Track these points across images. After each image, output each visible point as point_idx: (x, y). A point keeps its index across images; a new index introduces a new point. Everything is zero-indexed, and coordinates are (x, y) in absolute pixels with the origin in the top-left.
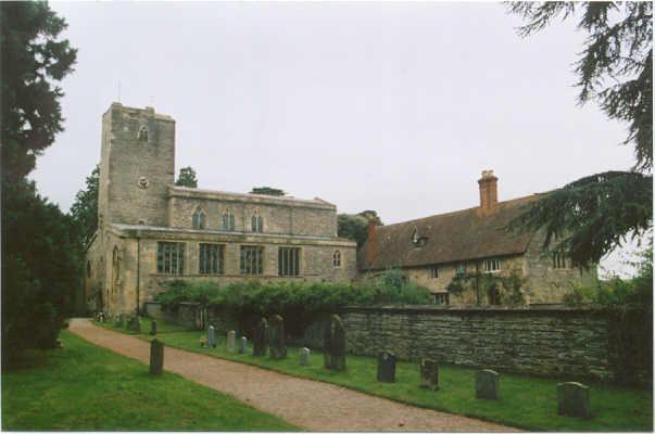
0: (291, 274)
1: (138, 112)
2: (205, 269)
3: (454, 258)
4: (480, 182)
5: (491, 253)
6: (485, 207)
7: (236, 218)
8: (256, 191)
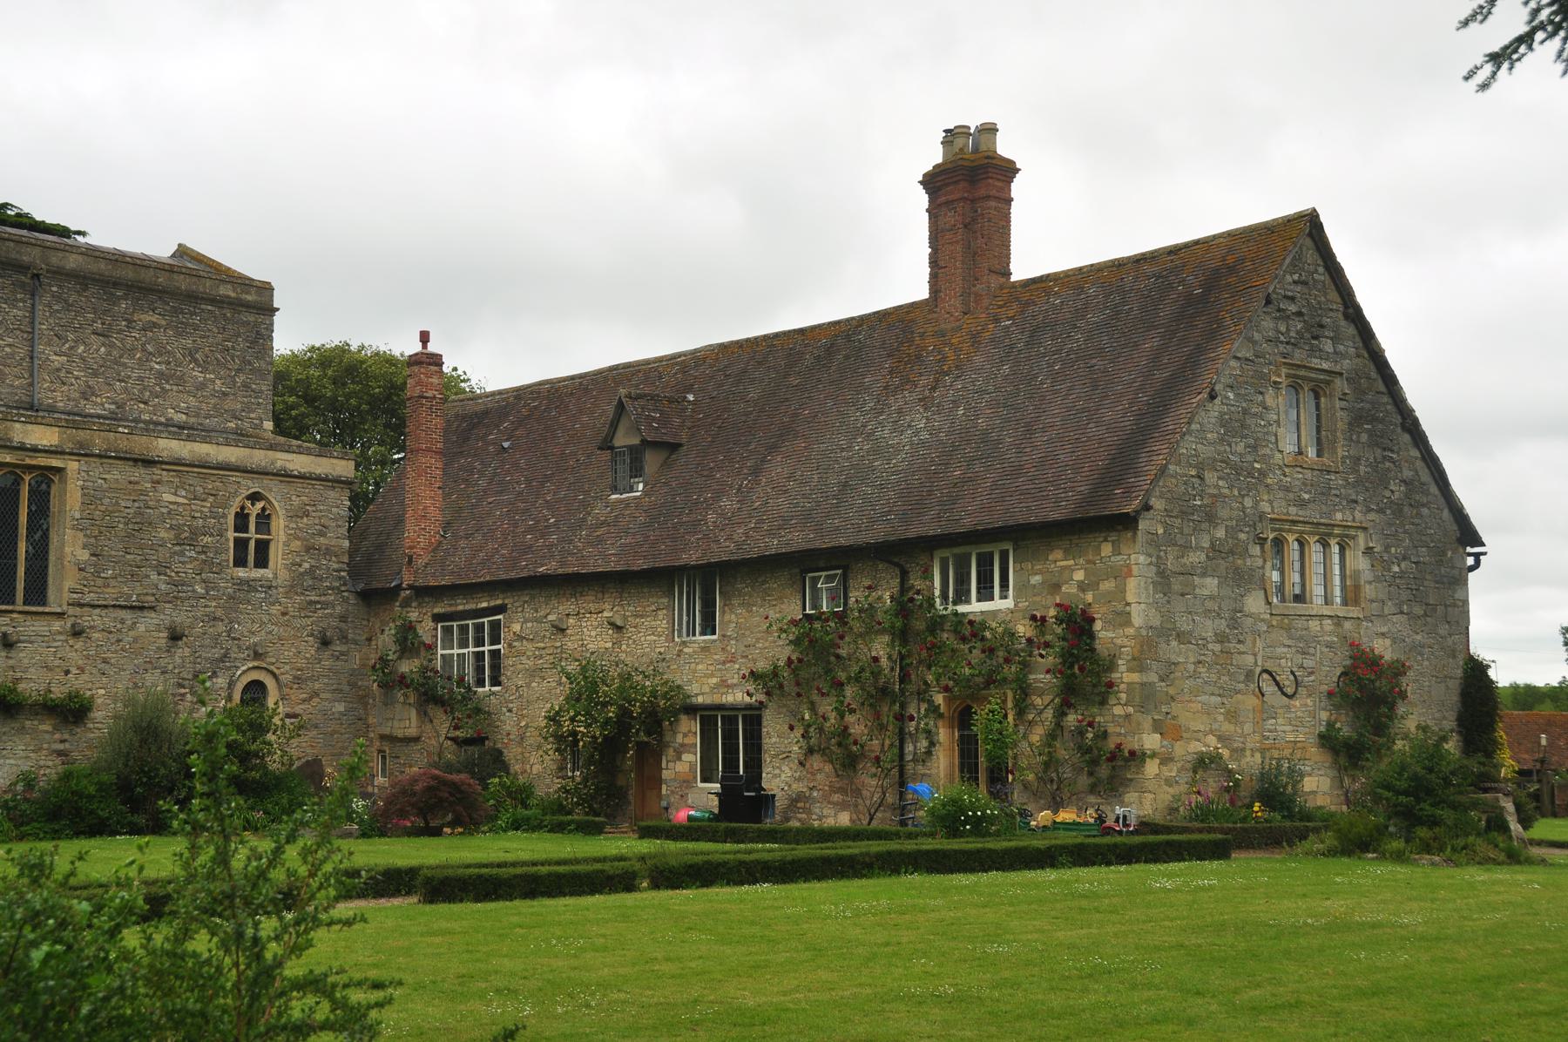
3: (797, 539)
4: (932, 182)
5: (968, 517)
6: (953, 303)
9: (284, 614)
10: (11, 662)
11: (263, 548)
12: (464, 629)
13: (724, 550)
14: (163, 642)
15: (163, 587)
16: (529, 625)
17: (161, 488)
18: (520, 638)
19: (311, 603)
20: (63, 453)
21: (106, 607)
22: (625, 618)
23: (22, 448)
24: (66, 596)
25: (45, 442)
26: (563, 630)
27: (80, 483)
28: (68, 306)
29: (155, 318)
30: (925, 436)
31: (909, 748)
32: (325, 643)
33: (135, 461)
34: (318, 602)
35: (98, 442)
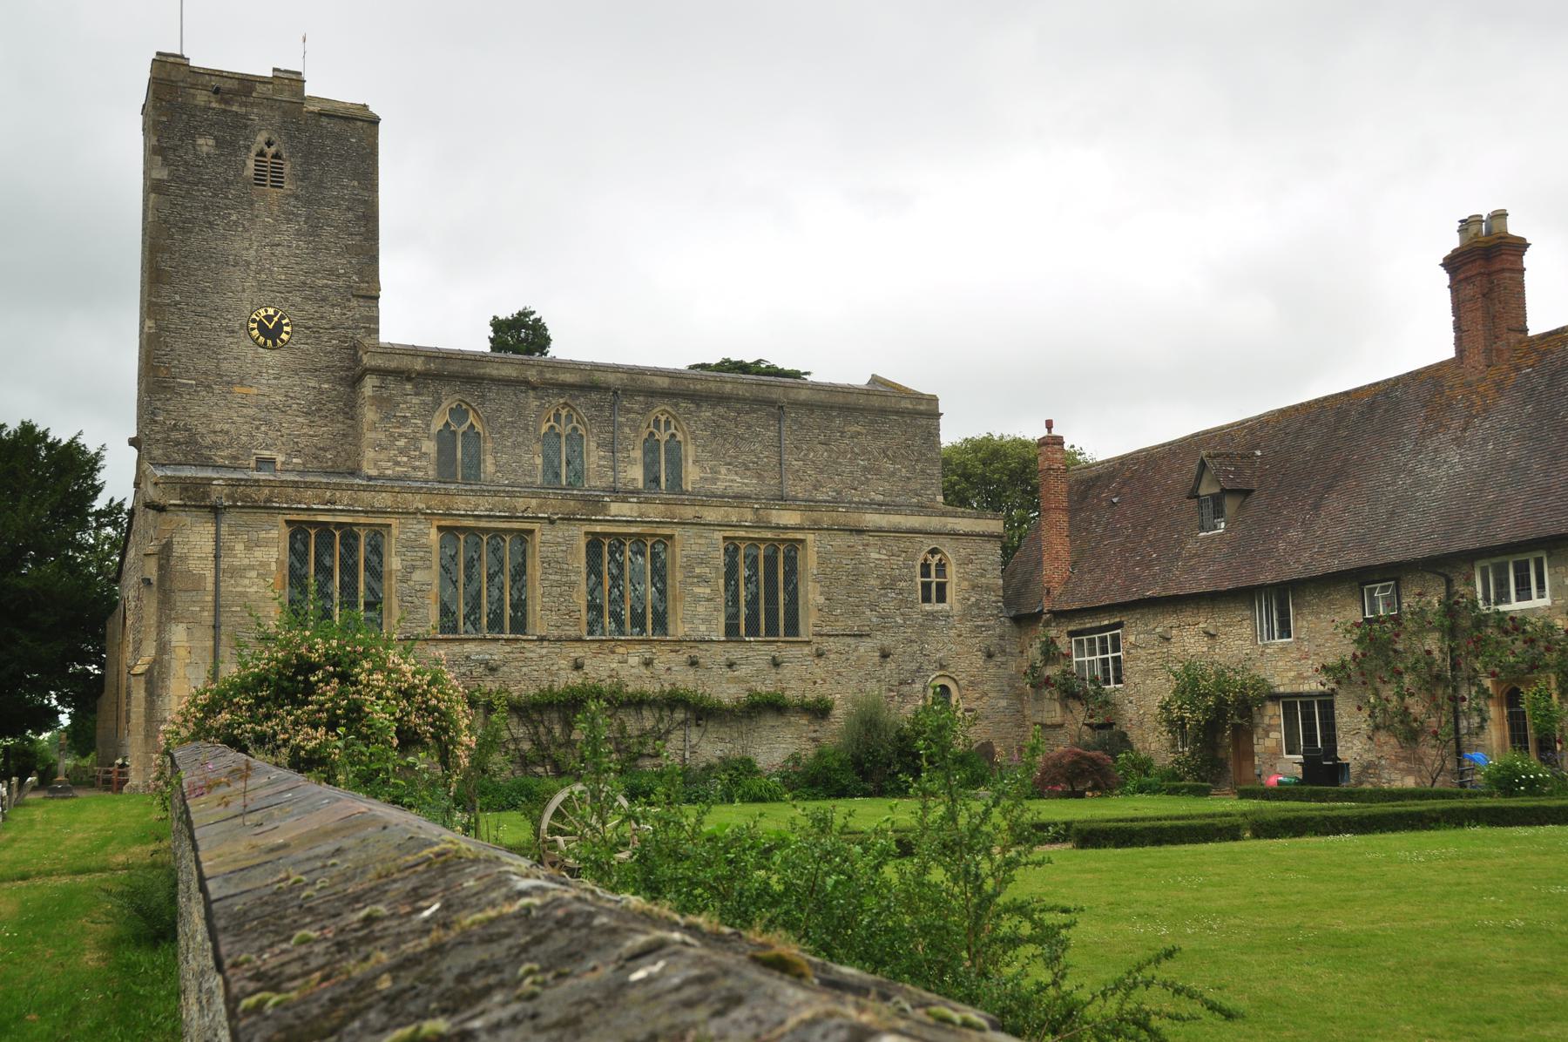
0: (772, 630)
1: (246, 84)
3: (1354, 559)
5: (1503, 533)
6: (1477, 359)
7: (591, 445)
9: (959, 636)
10: (779, 677)
11: (941, 588)
12: (1091, 642)
13: (1294, 571)
14: (877, 659)
15: (874, 620)
16: (1142, 636)
17: (869, 549)
18: (1135, 646)
19: (978, 626)
20: (803, 529)
21: (837, 635)
22: (1216, 627)
23: (778, 527)
24: (811, 629)
25: (792, 522)
26: (1168, 639)
27: (816, 549)
28: (802, 426)
29: (859, 429)
30: (1459, 468)
31: (1463, 723)
32: (990, 656)
33: (851, 531)
34: (983, 626)
35: (826, 519)
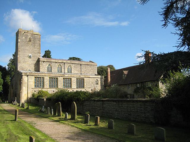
2: (51, 86)
8: (70, 59)
